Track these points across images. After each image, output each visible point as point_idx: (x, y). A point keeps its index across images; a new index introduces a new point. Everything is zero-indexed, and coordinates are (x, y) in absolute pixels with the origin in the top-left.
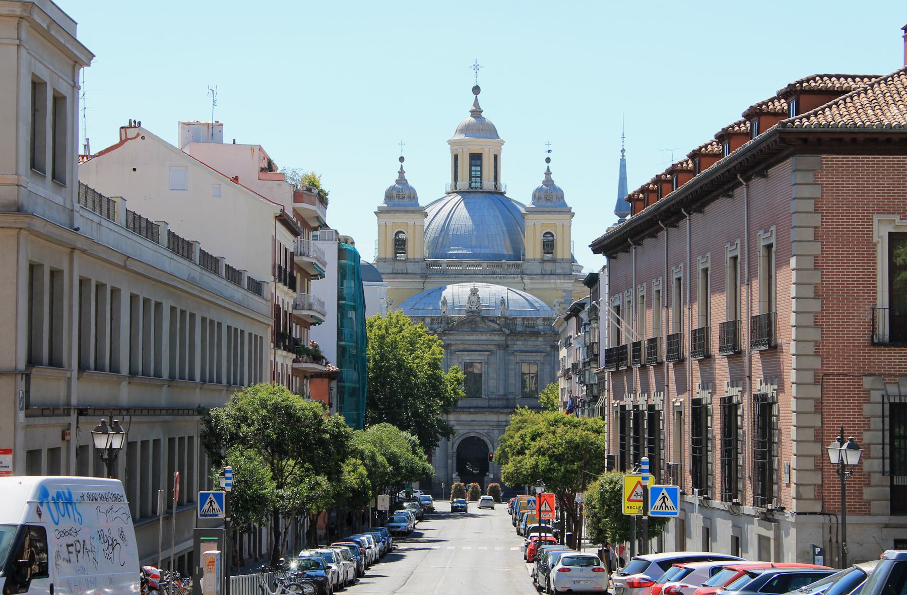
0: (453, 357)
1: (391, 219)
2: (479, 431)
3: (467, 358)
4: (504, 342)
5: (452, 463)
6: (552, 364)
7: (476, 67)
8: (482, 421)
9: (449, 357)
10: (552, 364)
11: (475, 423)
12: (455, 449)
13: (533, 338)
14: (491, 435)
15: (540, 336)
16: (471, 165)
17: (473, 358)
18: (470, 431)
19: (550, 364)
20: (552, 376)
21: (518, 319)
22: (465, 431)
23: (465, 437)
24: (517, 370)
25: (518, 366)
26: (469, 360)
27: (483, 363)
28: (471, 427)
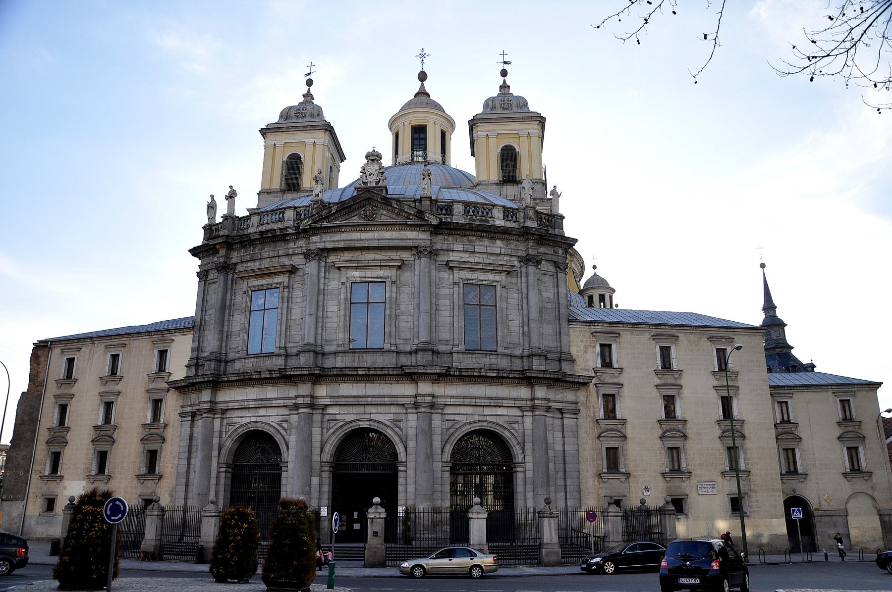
0: (331, 276)
1: (279, 139)
2: (381, 417)
3: (357, 274)
4: (428, 243)
5: (320, 485)
6: (524, 290)
7: (423, 56)
8: (384, 397)
9: (322, 274)
10: (524, 290)
11: (369, 399)
12: (327, 457)
13: (486, 242)
14: (403, 424)
15: (501, 239)
16: (413, 139)
17: (368, 275)
18: (359, 417)
19: (520, 291)
20: (525, 313)
21: (455, 206)
22: (353, 417)
23: (347, 429)
24: (456, 296)
25: (456, 289)
26: (360, 278)
27: (388, 283)
28: (359, 410)
